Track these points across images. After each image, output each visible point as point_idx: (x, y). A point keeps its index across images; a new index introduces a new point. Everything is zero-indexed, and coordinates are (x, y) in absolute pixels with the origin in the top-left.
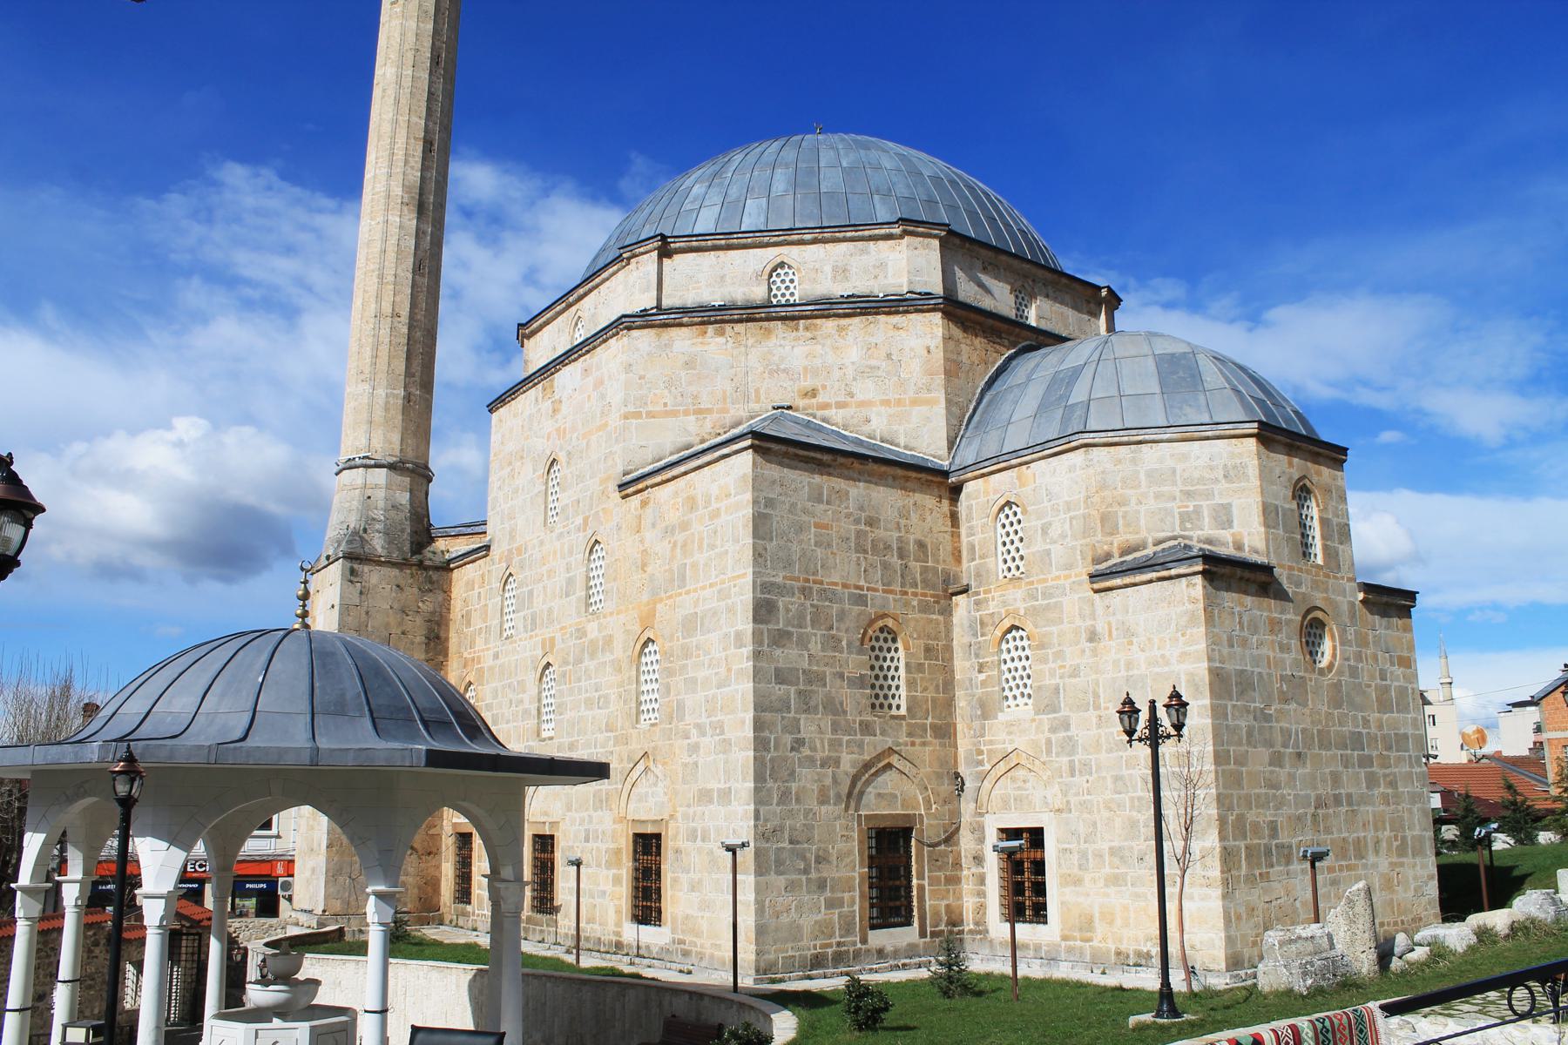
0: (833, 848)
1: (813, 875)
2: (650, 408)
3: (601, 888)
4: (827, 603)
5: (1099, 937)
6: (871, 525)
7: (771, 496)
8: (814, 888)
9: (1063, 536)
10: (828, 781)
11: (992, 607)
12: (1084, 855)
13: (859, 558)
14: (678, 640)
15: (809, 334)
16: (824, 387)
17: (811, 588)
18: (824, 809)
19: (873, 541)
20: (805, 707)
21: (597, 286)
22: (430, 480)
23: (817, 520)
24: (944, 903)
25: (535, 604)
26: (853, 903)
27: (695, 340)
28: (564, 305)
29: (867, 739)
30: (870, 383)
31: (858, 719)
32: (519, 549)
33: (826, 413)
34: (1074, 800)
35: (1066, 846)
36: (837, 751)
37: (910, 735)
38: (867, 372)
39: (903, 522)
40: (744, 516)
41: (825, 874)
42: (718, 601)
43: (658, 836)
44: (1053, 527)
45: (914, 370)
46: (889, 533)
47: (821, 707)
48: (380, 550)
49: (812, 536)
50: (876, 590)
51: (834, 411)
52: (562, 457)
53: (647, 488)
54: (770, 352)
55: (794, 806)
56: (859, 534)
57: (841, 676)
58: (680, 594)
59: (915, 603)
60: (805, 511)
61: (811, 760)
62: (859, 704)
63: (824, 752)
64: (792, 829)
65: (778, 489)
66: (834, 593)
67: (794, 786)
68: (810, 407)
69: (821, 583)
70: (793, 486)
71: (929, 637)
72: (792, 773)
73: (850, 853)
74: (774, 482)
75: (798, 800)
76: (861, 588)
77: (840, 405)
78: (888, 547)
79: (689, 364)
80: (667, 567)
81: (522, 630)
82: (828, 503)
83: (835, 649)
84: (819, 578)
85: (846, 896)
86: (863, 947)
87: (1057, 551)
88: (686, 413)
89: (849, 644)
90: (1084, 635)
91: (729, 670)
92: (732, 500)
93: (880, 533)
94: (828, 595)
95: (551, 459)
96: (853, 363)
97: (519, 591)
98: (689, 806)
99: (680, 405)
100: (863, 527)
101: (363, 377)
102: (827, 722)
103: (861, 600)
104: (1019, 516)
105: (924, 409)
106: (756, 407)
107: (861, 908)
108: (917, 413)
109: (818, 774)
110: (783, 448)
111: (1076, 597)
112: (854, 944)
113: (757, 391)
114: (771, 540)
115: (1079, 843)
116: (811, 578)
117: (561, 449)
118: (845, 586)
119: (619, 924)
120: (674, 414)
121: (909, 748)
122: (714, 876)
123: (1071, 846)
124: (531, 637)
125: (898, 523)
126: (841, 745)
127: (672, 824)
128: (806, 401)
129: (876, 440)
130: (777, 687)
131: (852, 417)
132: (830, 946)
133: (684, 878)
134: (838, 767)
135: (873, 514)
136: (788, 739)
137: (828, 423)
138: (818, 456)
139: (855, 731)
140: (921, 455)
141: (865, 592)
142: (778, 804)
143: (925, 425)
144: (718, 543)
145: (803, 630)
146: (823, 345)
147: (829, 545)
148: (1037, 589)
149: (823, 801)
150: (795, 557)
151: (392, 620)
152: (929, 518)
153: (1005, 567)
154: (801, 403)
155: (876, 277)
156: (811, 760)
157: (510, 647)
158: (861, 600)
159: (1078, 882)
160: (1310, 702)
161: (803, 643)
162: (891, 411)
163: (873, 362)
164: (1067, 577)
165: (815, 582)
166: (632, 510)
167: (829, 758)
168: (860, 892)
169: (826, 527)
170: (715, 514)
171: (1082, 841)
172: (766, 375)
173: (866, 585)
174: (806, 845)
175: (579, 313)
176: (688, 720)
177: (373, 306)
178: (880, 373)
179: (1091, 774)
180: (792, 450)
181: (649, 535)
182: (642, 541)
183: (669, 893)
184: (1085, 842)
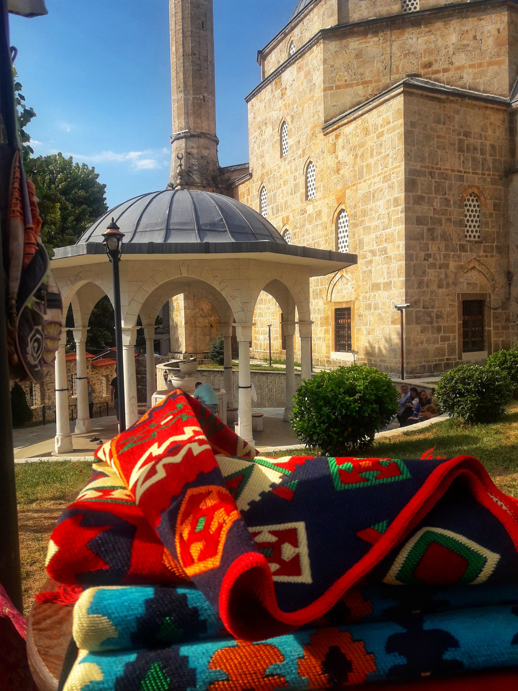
0: (445, 311)
1: (435, 324)
2: (338, 83)
3: (318, 336)
4: (443, 180)
6: (466, 136)
10: (443, 276)
13: (460, 155)
14: (359, 207)
15: (427, 29)
16: (436, 60)
17: (435, 172)
18: (440, 291)
19: (467, 145)
20: (432, 237)
22: (217, 144)
23: (438, 134)
24: (501, 339)
25: (278, 200)
26: (455, 339)
27: (361, 41)
30: (463, 55)
31: (459, 243)
33: (437, 76)
36: (447, 260)
37: (485, 251)
38: (461, 48)
39: (483, 133)
40: (398, 133)
42: (383, 182)
43: (349, 309)
45: (489, 43)
46: (476, 140)
47: (439, 237)
50: (469, 173)
52: (288, 119)
54: (404, 43)
55: (425, 289)
56: (461, 141)
57: (450, 220)
58: (360, 183)
59: (489, 180)
60: (432, 129)
63: (441, 260)
64: (424, 301)
66: (447, 175)
67: (426, 279)
68: (428, 73)
69: (440, 169)
70: (425, 115)
71: (496, 199)
72: (424, 272)
73: (453, 313)
74: (415, 112)
75: (427, 286)
76: (461, 172)
77: (445, 70)
78: (475, 149)
79: (358, 56)
80: (352, 169)
81: (271, 214)
82: (444, 124)
84: (439, 166)
85: (452, 335)
86: (460, 361)
88: (357, 84)
89: (454, 203)
91: (390, 219)
92: (391, 125)
93: (472, 140)
94: (444, 176)
95: (282, 122)
96: (453, 44)
97: (268, 195)
98: (367, 292)
99: (354, 80)
100: (462, 137)
102: (442, 246)
103: (461, 179)
105: (496, 68)
106: (397, 76)
109: (438, 272)
110: (420, 92)
112: (455, 359)
113: (397, 67)
114: (414, 145)
116: (435, 166)
118: (453, 171)
119: (328, 352)
121: (484, 258)
124: (276, 217)
125: (481, 135)
126: (450, 257)
127: (357, 303)
128: (426, 70)
129: (466, 89)
130: (417, 226)
131: (452, 77)
132: (443, 360)
133: (364, 329)
134: (448, 269)
135: (468, 130)
137: (439, 82)
138: (439, 96)
139: (457, 250)
140: (493, 95)
141: (463, 174)
142: (417, 289)
143: (496, 77)
144: (383, 151)
146: (435, 35)
147: (444, 148)
149: (440, 286)
152: (498, 131)
154: (422, 72)
158: (461, 178)
162: (476, 71)
163: (465, 42)
165: (437, 169)
166: (330, 140)
167: (443, 264)
168: (459, 333)
170: (382, 134)
173: (464, 170)
174: (431, 309)
176: (366, 248)
177: (181, 50)
178: (469, 48)
180: (425, 93)
182: (337, 157)
183: (356, 336)
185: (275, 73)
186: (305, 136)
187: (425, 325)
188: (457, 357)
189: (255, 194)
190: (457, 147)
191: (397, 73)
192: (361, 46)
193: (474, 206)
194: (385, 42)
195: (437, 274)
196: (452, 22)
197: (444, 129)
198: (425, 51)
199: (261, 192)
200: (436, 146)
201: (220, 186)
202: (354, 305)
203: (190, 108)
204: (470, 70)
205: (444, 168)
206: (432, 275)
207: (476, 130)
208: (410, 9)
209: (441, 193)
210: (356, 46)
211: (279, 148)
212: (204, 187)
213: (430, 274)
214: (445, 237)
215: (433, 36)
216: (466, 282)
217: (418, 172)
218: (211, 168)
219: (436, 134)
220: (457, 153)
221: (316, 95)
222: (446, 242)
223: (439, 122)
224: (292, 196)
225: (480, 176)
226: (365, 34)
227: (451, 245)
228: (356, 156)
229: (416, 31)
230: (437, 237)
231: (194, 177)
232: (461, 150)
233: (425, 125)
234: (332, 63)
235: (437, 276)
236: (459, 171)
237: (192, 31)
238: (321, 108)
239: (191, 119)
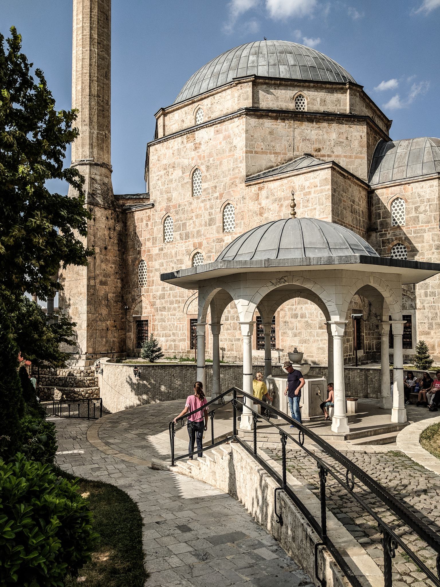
2: (256, 149)
5: (437, 352)
9: (425, 211)
11: (388, 236)
12: (431, 324)
15: (317, 126)
16: (323, 148)
21: (213, 95)
25: (187, 229)
28: (191, 102)
30: (340, 148)
32: (175, 206)
34: (426, 305)
35: (422, 321)
44: (421, 208)
45: (356, 144)
48: (100, 202)
51: (327, 158)
53: (264, 182)
77: (329, 156)
79: (271, 133)
80: (277, 214)
87: (422, 216)
88: (270, 153)
90: (434, 247)
95: (195, 168)
101: (85, 123)
104: (402, 203)
105: (359, 160)
106: (298, 153)
108: (357, 161)
111: (431, 233)
113: (298, 147)
115: (429, 320)
117: (202, 164)
120: (266, 153)
122: (308, 330)
123: (425, 321)
128: (316, 153)
148: (411, 230)
151: (106, 233)
153: (394, 222)
154: (315, 154)
155: (336, 105)
157: (171, 246)
159: (428, 333)
162: (348, 160)
163: (341, 140)
164: (426, 226)
171: (430, 319)
172: (301, 141)
175: (199, 106)
177: (88, 90)
178: (344, 145)
179: (435, 296)
181: (264, 202)
184: (432, 320)
185: (189, 130)
186: (223, 184)
189: (157, 221)
191: (298, 151)
192: (273, 126)
194: (290, 127)
196: (333, 125)
198: (316, 140)
199: (165, 220)
201: (117, 209)
202: (279, 314)
203: (94, 141)
204: (344, 159)
207: (357, 200)
208: (300, 109)
210: (270, 126)
211: (191, 189)
212: (105, 209)
215: (321, 131)
218: (110, 194)
221: (236, 154)
224: (206, 228)
226: (276, 118)
228: (282, 205)
229: (310, 125)
231: (97, 199)
234: (252, 134)
237: (98, 78)
238: (243, 166)
239: (95, 150)
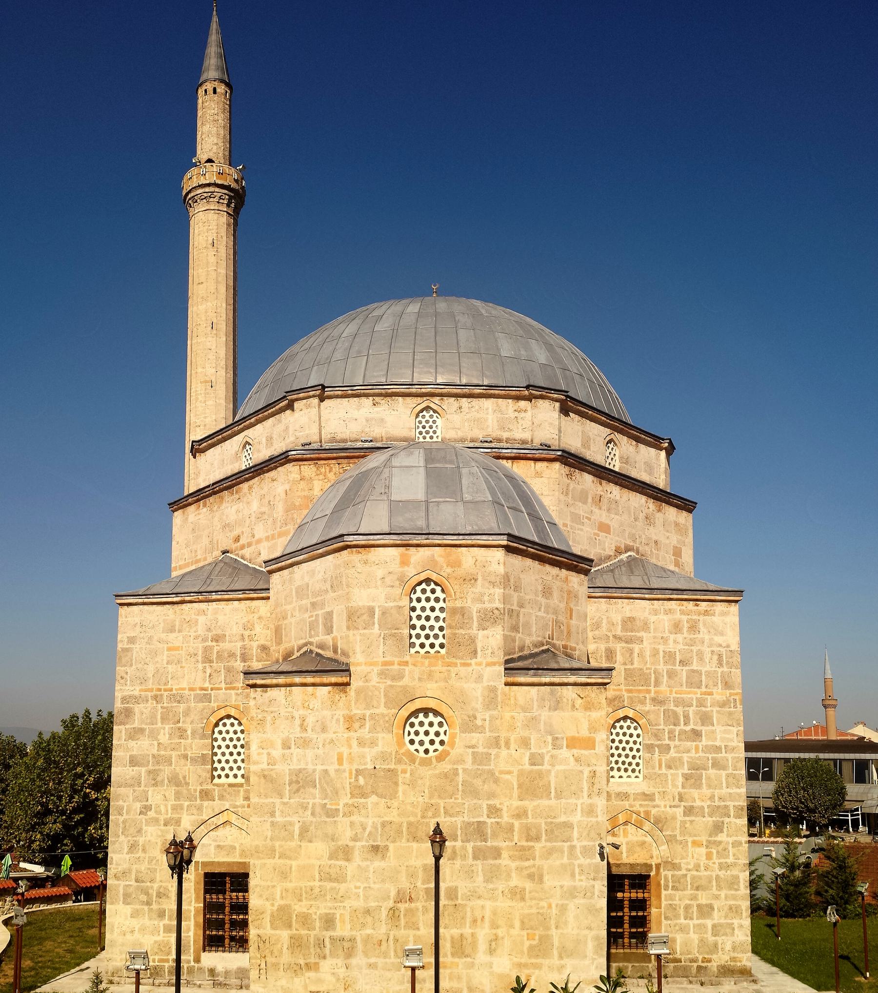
1: (155, 906)
4: (175, 704)
7: (132, 635)
8: (155, 916)
17: (162, 695)
19: (218, 652)
20: (153, 782)
23: (170, 645)
29: (206, 803)
31: (199, 788)
36: (178, 813)
41: (164, 906)
49: (165, 657)
55: (140, 854)
56: (206, 649)
61: (157, 820)
62: (200, 776)
63: (167, 814)
64: (137, 871)
65: (138, 629)
69: (171, 690)
70: (150, 625)
72: (140, 831)
75: (144, 850)
83: (181, 737)
84: (169, 686)
86: (196, 965)
89: (194, 733)
102: (171, 792)
103: (207, 698)
107: (195, 934)
109: (161, 831)
114: (131, 665)
116: (163, 687)
118: (191, 689)
121: (246, 809)
126: (182, 809)
134: (179, 826)
136: (138, 806)
141: (209, 692)
145: (153, 726)
150: (150, 675)
156: (157, 820)
158: (207, 698)
160: (400, 794)
161: (154, 735)
167: (171, 819)
168: (195, 922)
169: (176, 649)
173: (210, 686)
187: (138, 907)
188: (192, 958)
190: (200, 658)
193: (235, 732)
195: (160, 833)
197: (181, 638)
200: (165, 662)
205: (177, 687)
206: (152, 835)
209: (171, 722)
213: (149, 834)
214: (176, 781)
216: (214, 844)
217: (136, 698)
219: (166, 646)
220: (200, 666)
222: (176, 788)
223: (172, 630)
225: (240, 691)
227: (185, 792)
230: (163, 781)
232: (208, 660)
233: (151, 638)
235: (160, 836)
236: (202, 689)
